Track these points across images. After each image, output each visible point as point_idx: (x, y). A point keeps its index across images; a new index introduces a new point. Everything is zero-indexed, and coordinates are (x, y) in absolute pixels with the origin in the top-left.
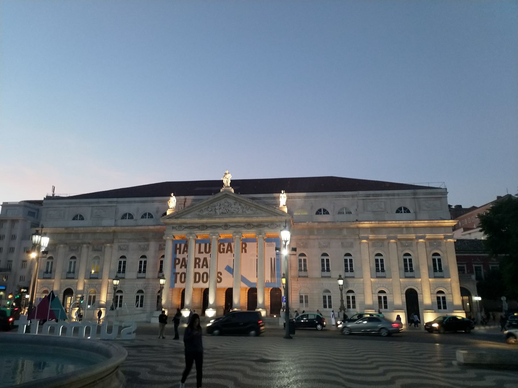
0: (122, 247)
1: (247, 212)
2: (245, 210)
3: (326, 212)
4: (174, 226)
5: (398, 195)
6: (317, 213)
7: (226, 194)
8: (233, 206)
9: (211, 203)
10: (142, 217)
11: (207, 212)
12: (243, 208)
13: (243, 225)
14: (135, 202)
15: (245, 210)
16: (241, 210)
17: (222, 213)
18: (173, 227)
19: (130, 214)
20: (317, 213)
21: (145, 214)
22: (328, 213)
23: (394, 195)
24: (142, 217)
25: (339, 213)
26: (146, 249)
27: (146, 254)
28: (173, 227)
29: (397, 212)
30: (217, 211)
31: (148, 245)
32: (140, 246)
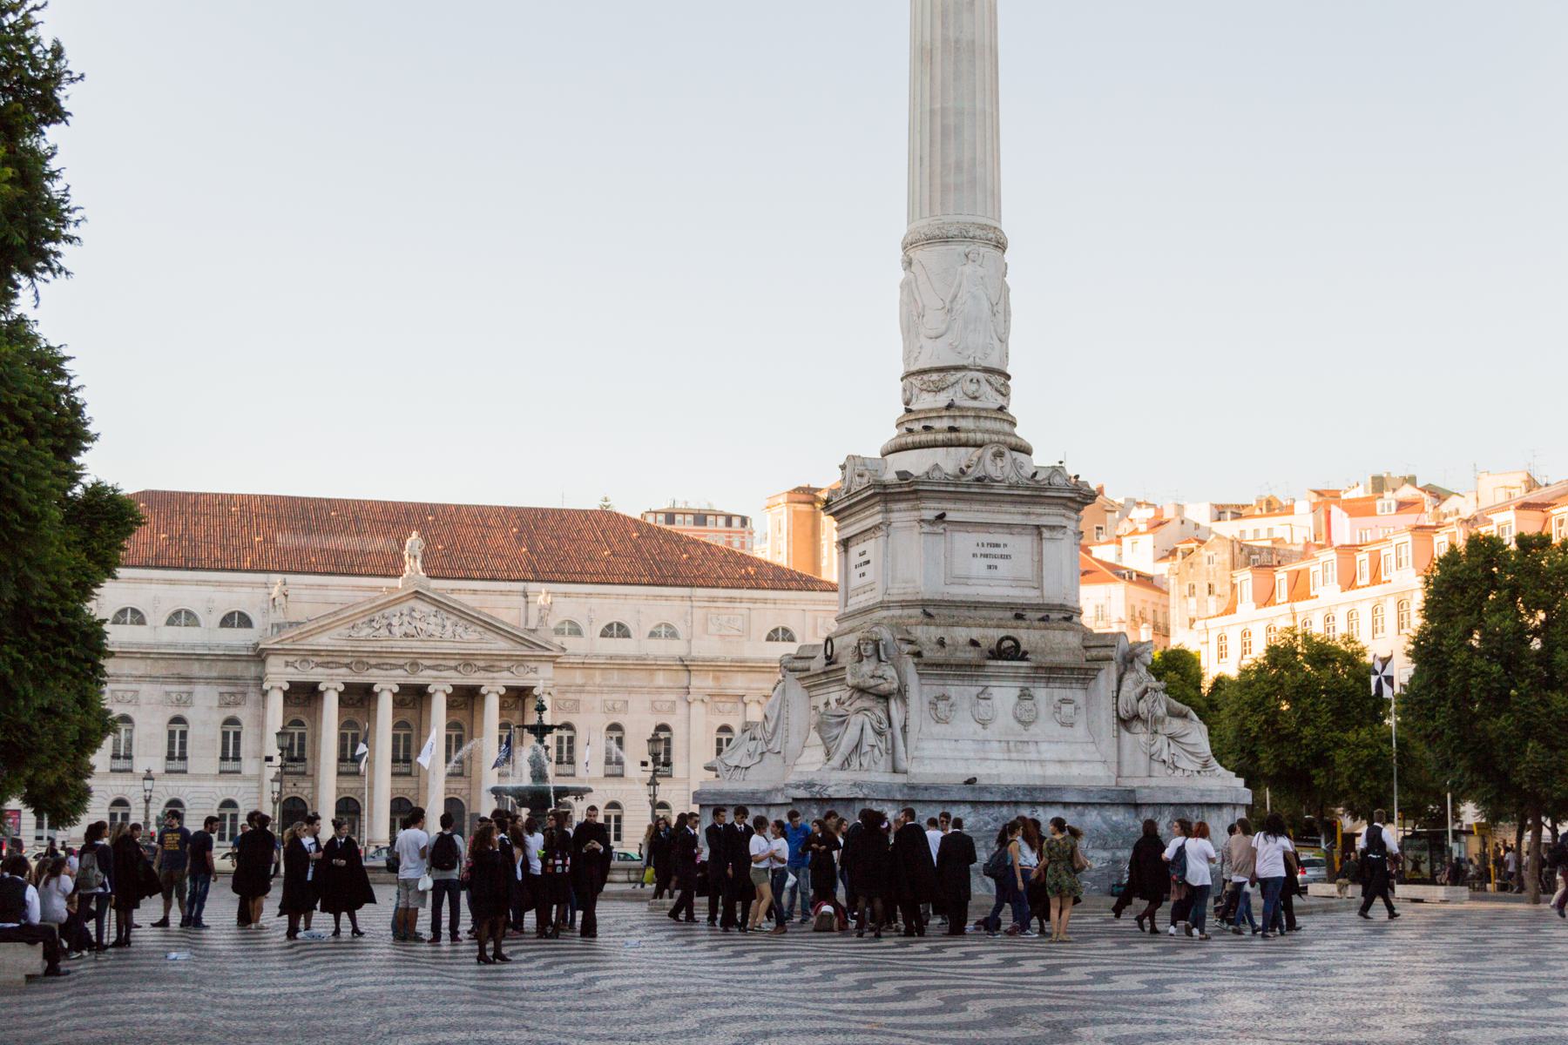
0: (120, 694)
3: (622, 631)
5: (775, 602)
6: (603, 635)
8: (432, 620)
10: (170, 623)
13: (453, 663)
14: (150, 581)
15: (460, 630)
17: (406, 635)
19: (135, 611)
20: (603, 635)
21: (177, 614)
22: (627, 635)
23: (765, 601)
24: (170, 623)
25: (652, 635)
26: (185, 701)
27: (187, 713)
29: (769, 639)
30: (395, 630)
31: (190, 693)
32: (168, 693)
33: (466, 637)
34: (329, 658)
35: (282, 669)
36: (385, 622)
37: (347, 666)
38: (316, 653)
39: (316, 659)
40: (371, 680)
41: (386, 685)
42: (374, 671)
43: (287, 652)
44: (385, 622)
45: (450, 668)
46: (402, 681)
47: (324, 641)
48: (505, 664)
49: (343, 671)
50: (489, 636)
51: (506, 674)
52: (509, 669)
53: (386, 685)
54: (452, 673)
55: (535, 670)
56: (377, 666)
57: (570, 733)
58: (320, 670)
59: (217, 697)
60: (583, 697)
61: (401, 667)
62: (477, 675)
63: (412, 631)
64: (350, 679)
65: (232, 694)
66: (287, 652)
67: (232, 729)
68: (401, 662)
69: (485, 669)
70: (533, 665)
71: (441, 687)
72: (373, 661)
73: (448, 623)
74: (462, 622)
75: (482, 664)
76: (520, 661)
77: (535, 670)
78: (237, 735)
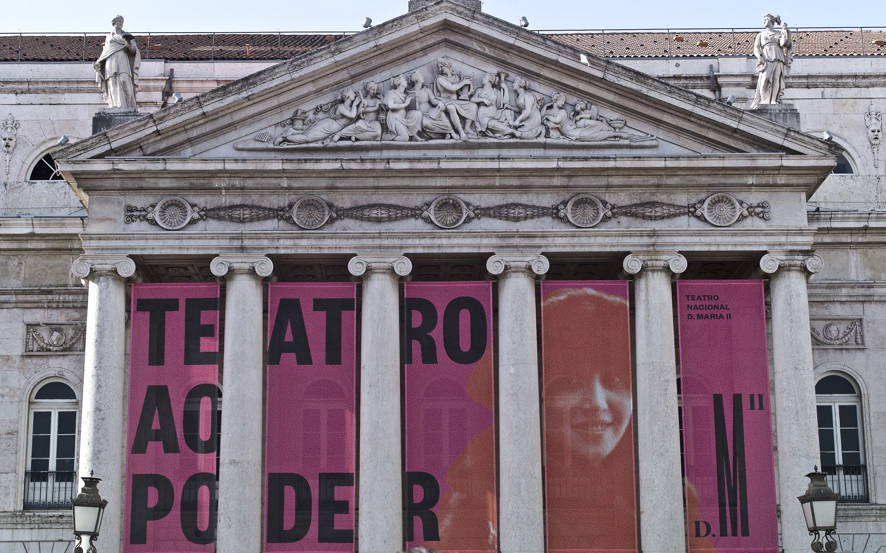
1: (569, 128)
2: (558, 116)
4: (139, 201)
7: (446, 25)
8: (488, 94)
9: (354, 78)
11: (335, 126)
12: (546, 105)
13: (547, 200)
15: (558, 116)
16: (537, 117)
17: (424, 132)
18: (130, 209)
28: (130, 209)
30: (395, 121)
33: (574, 133)
34: (238, 200)
35: (119, 226)
36: (371, 104)
37: (279, 213)
38: (202, 182)
39: (202, 200)
40: (344, 246)
41: (381, 263)
42: (350, 225)
43: (133, 183)
44: (371, 104)
45: (540, 212)
46: (421, 247)
47: (221, 154)
48: (682, 199)
49: (271, 225)
50: (636, 130)
51: (683, 222)
52: (691, 211)
53: (381, 263)
54: (546, 224)
55: (761, 211)
56: (357, 212)
57: (846, 400)
58: (213, 226)
59: (21, 330)
60: (871, 312)
61: (415, 213)
62: (611, 226)
63: (435, 120)
64: (287, 247)
65: (55, 328)
66: (133, 183)
67: (55, 407)
68: (416, 200)
69: (630, 211)
70: (754, 198)
71: (518, 260)
72: (344, 201)
73: (528, 100)
74: (561, 98)
75: (622, 199)
76: (719, 187)
77: (761, 211)
78: (69, 422)
